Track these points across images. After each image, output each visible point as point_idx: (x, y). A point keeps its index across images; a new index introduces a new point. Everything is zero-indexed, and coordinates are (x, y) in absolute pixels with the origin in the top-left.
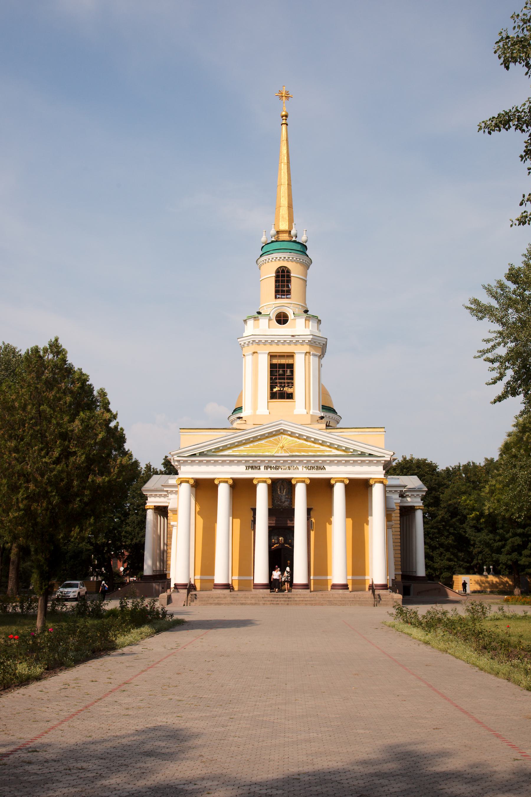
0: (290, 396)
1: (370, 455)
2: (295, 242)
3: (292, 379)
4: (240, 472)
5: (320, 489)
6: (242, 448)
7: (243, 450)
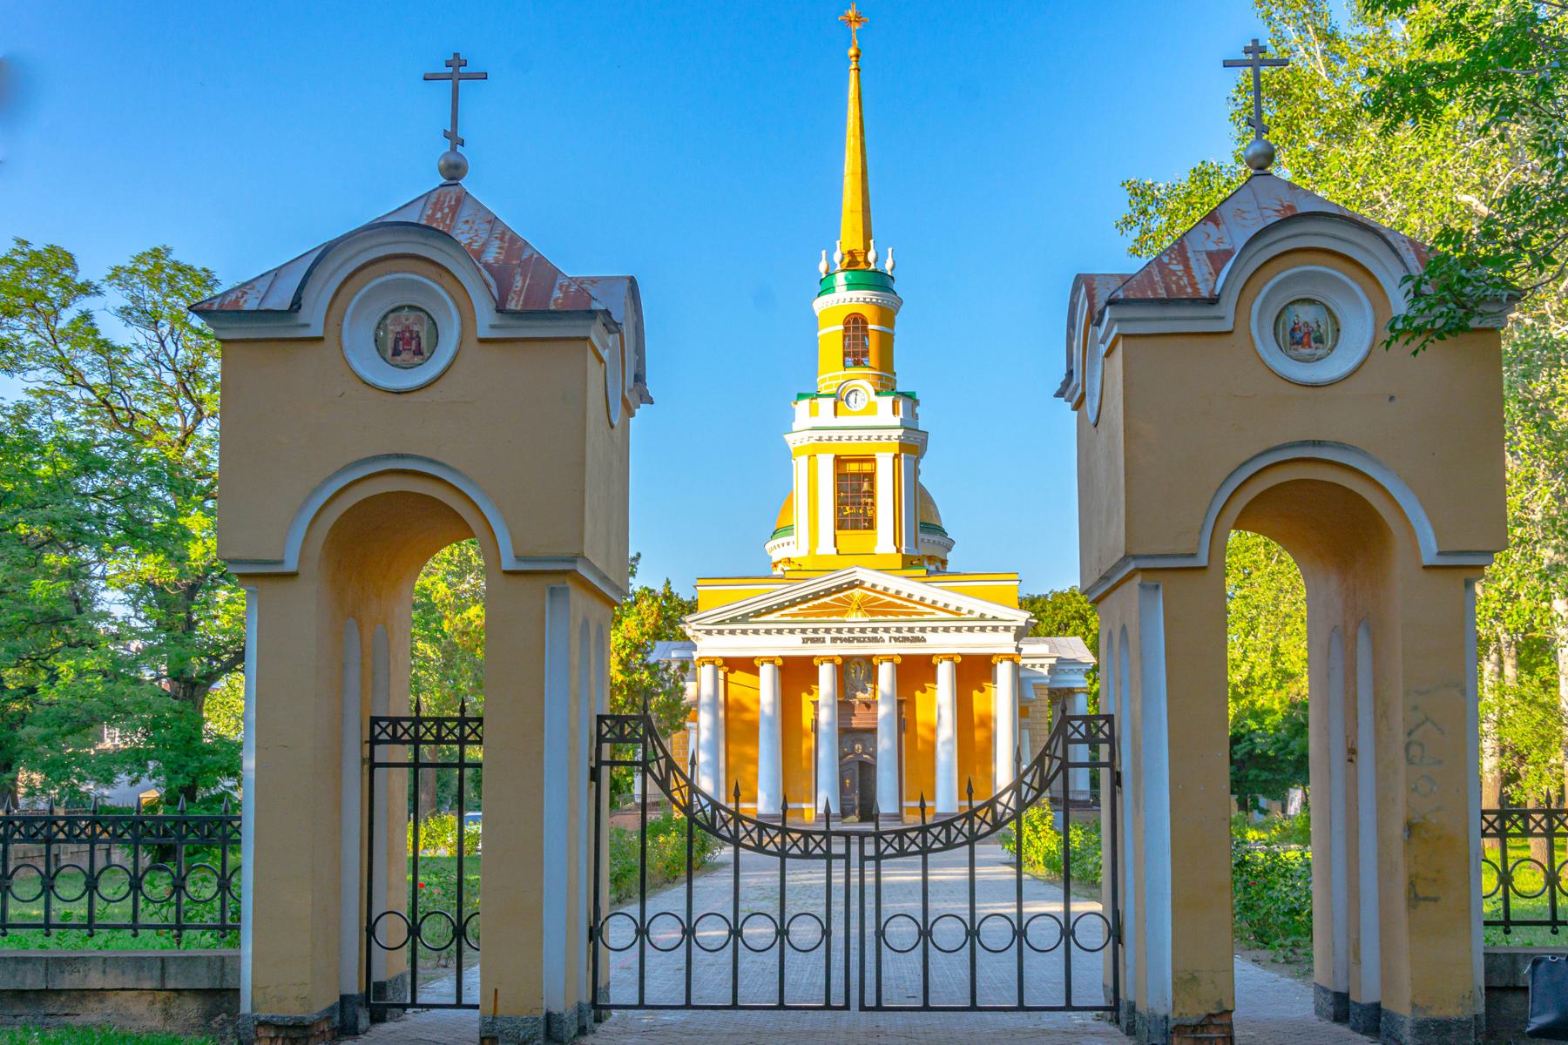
1: (994, 618)
2: (875, 271)
4: (792, 645)
5: (915, 672)
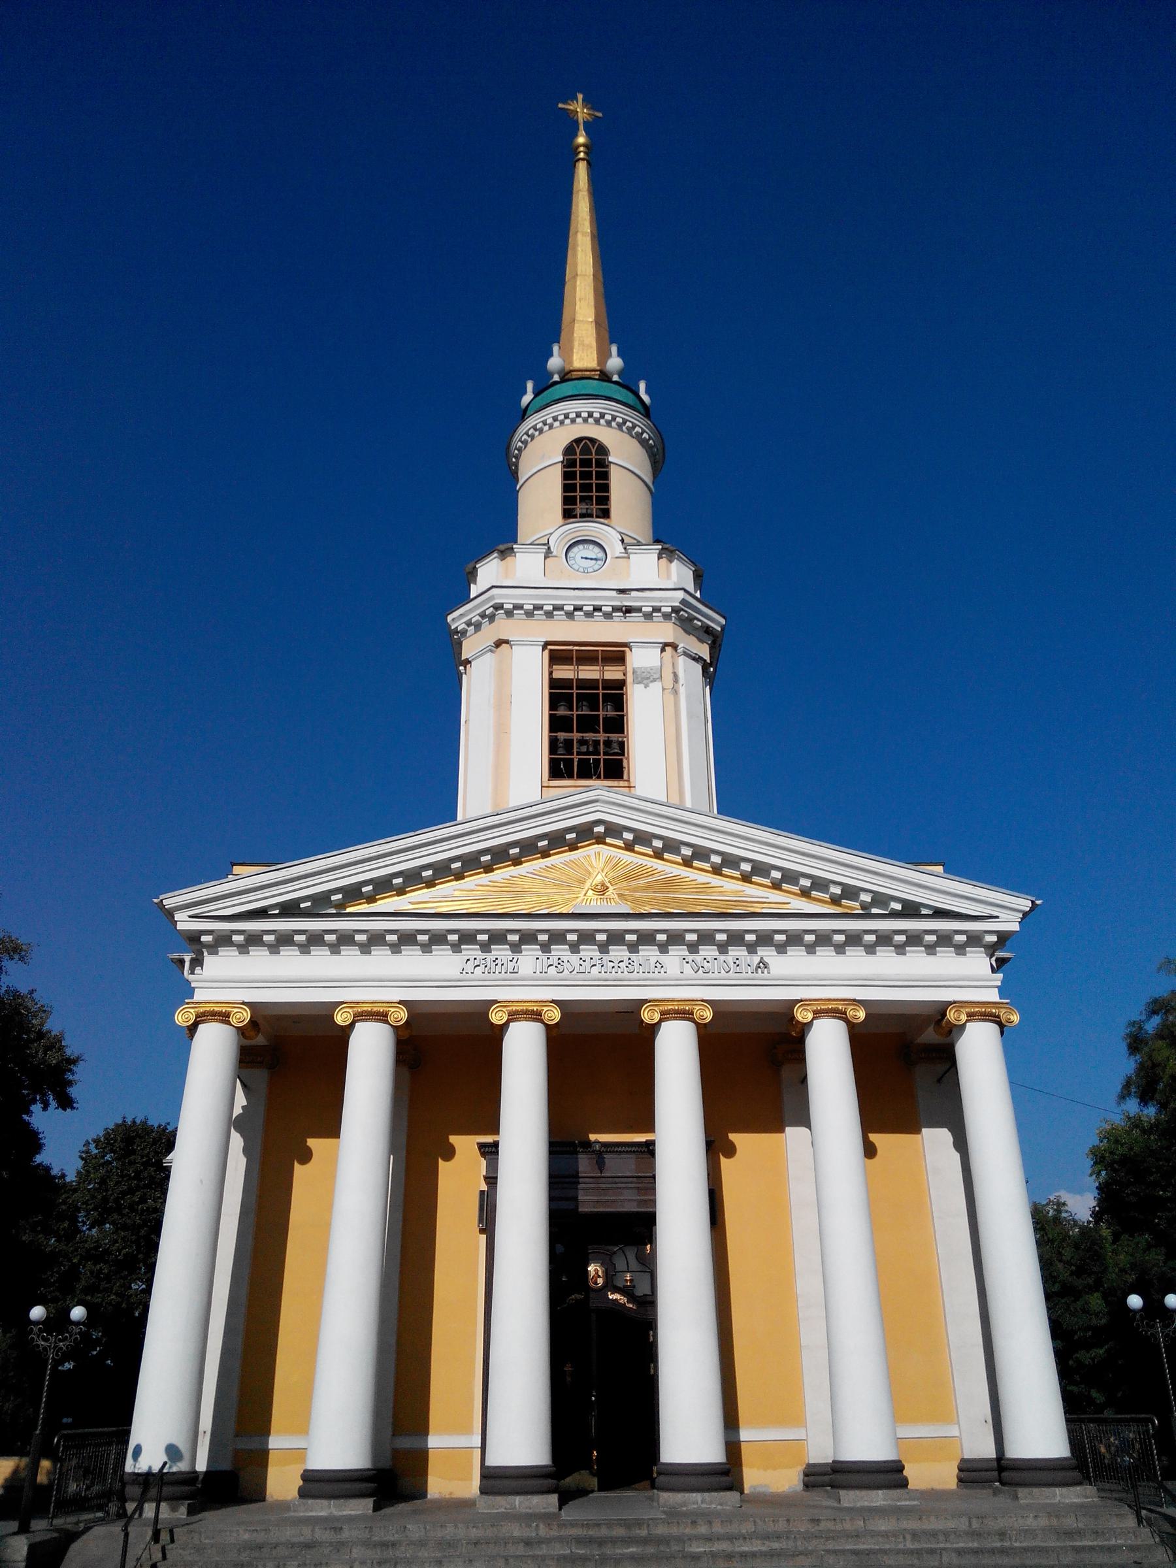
1: (940, 914)
4: (440, 978)
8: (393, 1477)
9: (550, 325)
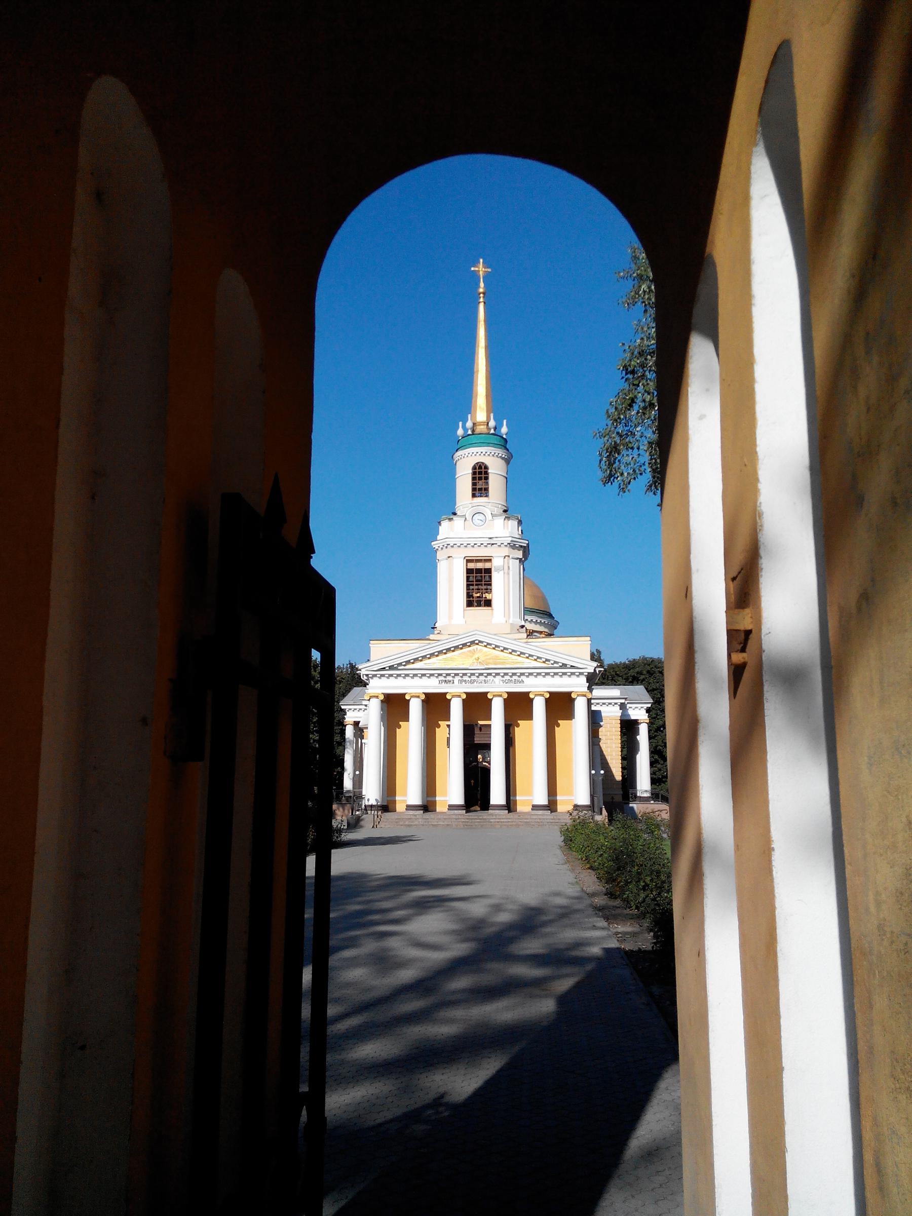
0: (488, 603)
1: (572, 667)
3: (490, 585)
4: (433, 686)
5: (518, 705)
6: (434, 660)
7: (435, 662)
8: (427, 807)
9: (468, 406)
